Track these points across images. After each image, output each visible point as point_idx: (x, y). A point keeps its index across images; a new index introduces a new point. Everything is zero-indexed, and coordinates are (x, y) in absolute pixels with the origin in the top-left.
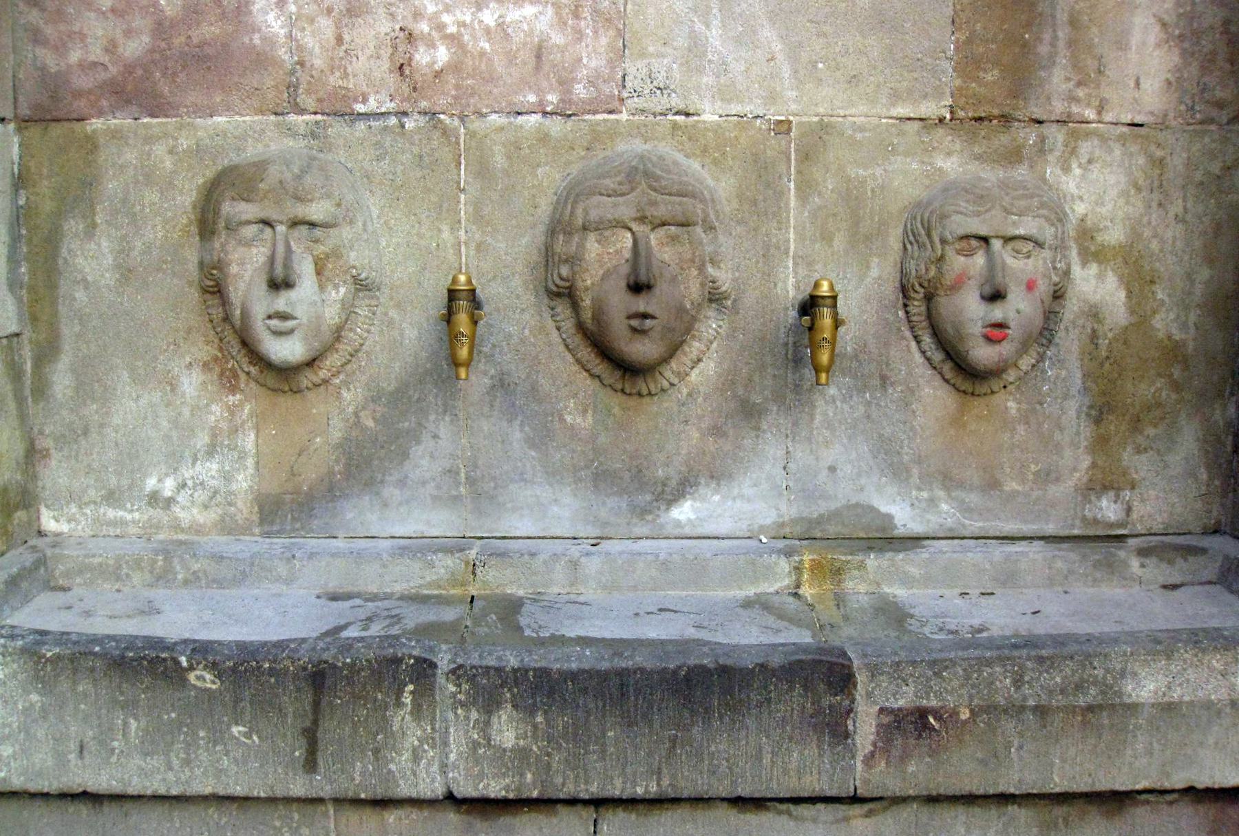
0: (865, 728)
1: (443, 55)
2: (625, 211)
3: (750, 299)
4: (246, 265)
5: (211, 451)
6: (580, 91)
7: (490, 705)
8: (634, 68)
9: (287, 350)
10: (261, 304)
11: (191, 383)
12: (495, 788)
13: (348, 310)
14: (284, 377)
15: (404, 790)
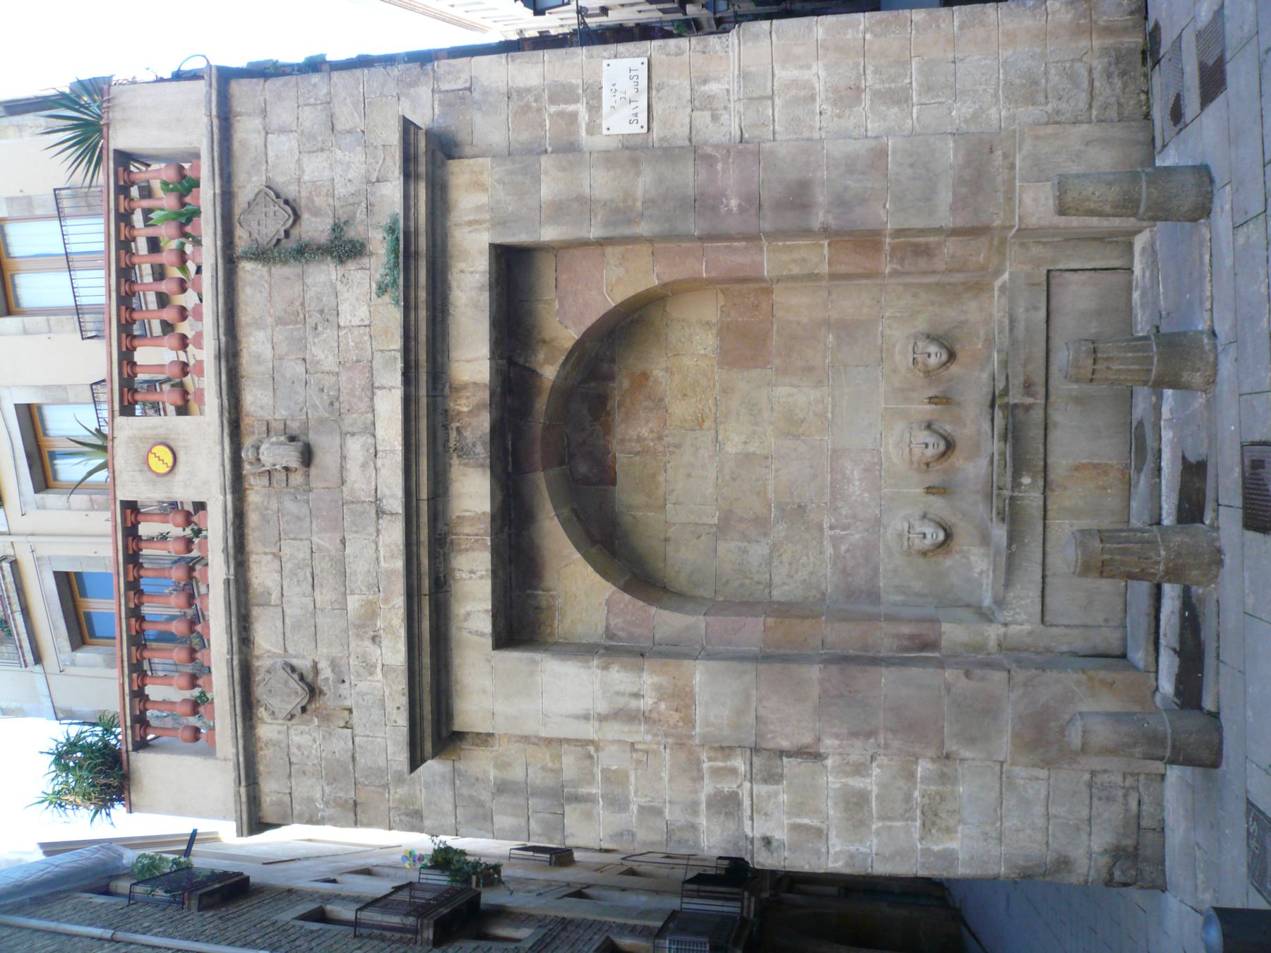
0: (1030, 400)
1: (866, 495)
2: (907, 450)
3: (928, 417)
4: (918, 544)
5: (968, 558)
6: (876, 460)
7: (1020, 484)
8: (870, 446)
9: (941, 536)
10: (929, 541)
11: (948, 562)
12: (1041, 483)
13: (931, 520)
14: (949, 536)
15: (1041, 503)
